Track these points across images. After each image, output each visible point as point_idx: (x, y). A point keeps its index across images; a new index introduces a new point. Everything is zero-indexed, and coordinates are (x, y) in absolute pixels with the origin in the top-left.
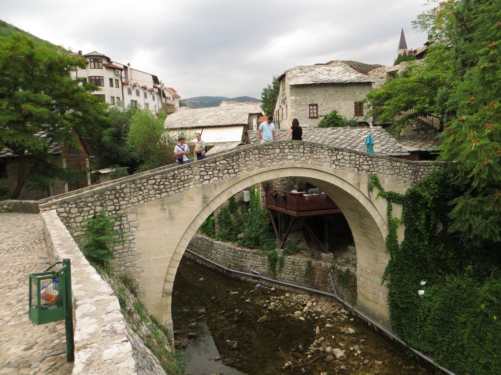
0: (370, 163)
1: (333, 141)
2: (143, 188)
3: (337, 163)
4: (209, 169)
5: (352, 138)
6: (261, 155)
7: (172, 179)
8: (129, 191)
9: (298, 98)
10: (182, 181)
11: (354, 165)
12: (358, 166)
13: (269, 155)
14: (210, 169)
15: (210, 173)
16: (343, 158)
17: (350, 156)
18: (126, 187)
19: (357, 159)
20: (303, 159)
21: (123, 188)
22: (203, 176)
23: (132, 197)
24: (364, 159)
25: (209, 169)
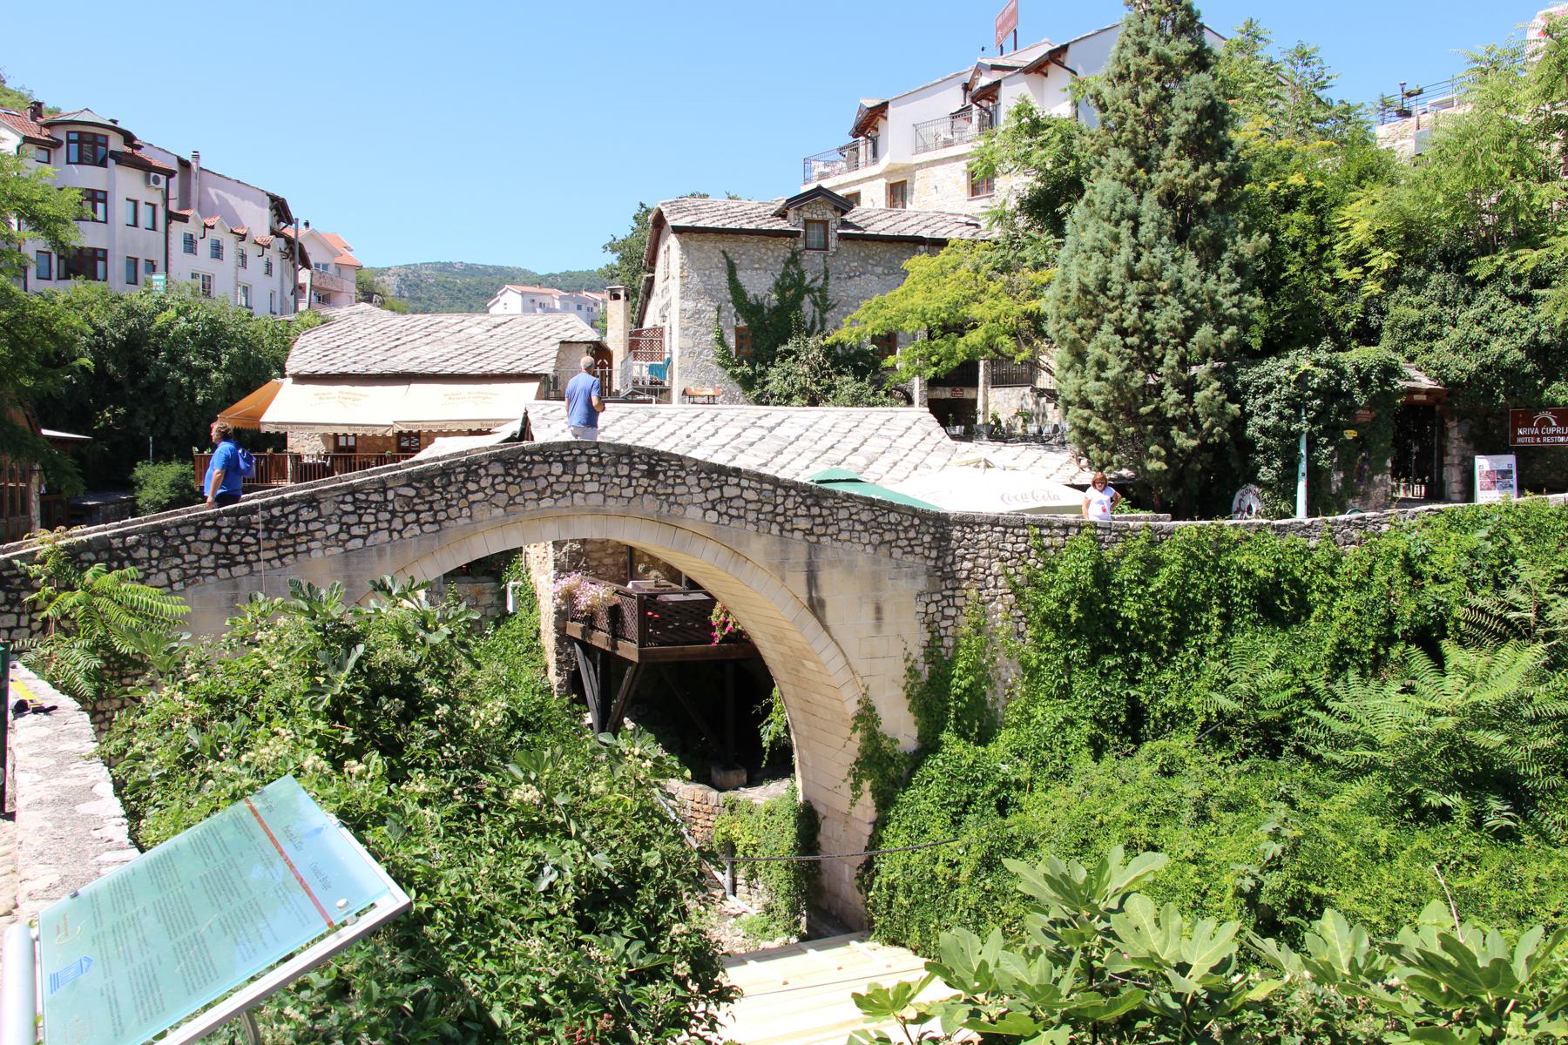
0: (815, 511)
2: (184, 549)
3: (722, 508)
6: (510, 479)
11: (769, 517)
12: (780, 519)
13: (534, 479)
14: (369, 507)
15: (368, 519)
16: (740, 497)
17: (760, 491)
18: (139, 543)
21: (131, 547)
22: (349, 526)
23: (154, 570)
24: (799, 500)
25: (366, 509)
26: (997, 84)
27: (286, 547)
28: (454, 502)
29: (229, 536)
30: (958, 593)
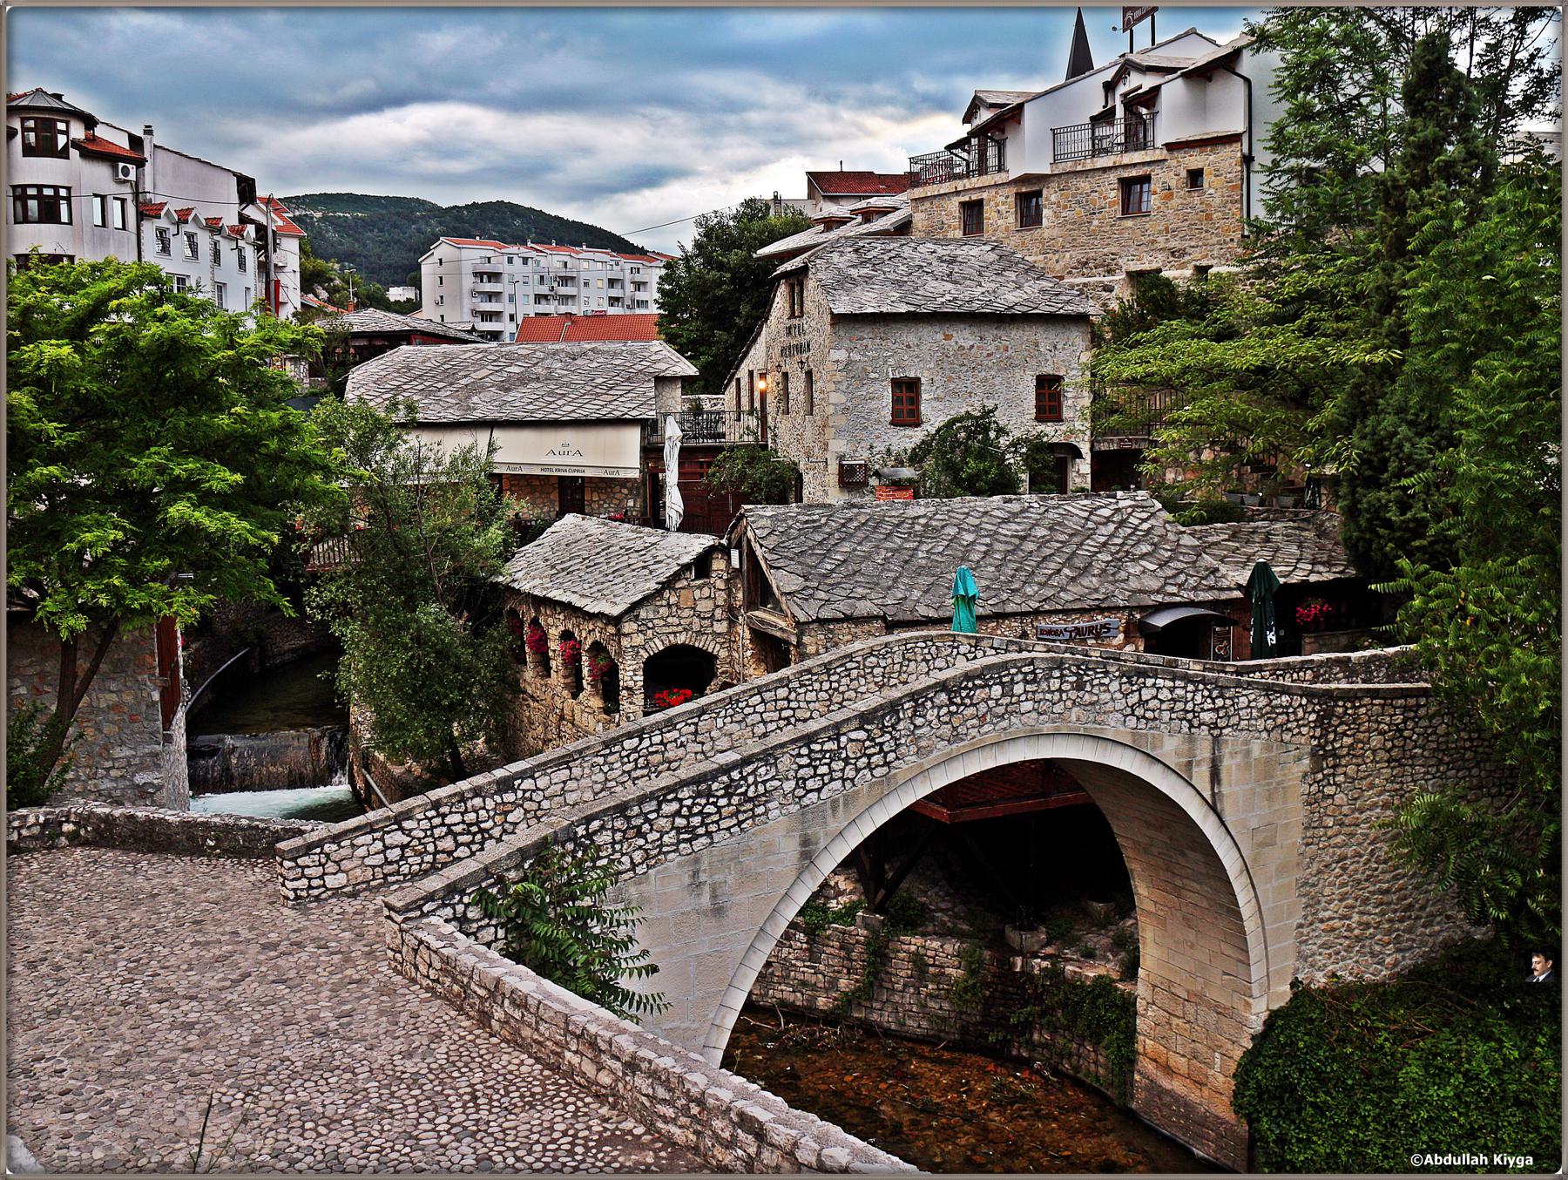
0: (1220, 702)
1: (1018, 547)
2: (646, 827)
4: (820, 760)
5: (1071, 535)
6: (953, 708)
7: (722, 797)
8: (609, 839)
9: (858, 358)
10: (751, 800)
11: (1181, 715)
12: (1190, 716)
13: (975, 705)
14: (824, 757)
15: (823, 770)
16: (1155, 697)
18: (602, 828)
19: (1190, 696)
20: (1058, 708)
21: (595, 832)
22: (805, 780)
23: (617, 856)
24: (1206, 693)
25: (820, 760)
26: (1156, 90)
27: (745, 812)
28: (903, 741)
29: (690, 808)
30: (1340, 770)
